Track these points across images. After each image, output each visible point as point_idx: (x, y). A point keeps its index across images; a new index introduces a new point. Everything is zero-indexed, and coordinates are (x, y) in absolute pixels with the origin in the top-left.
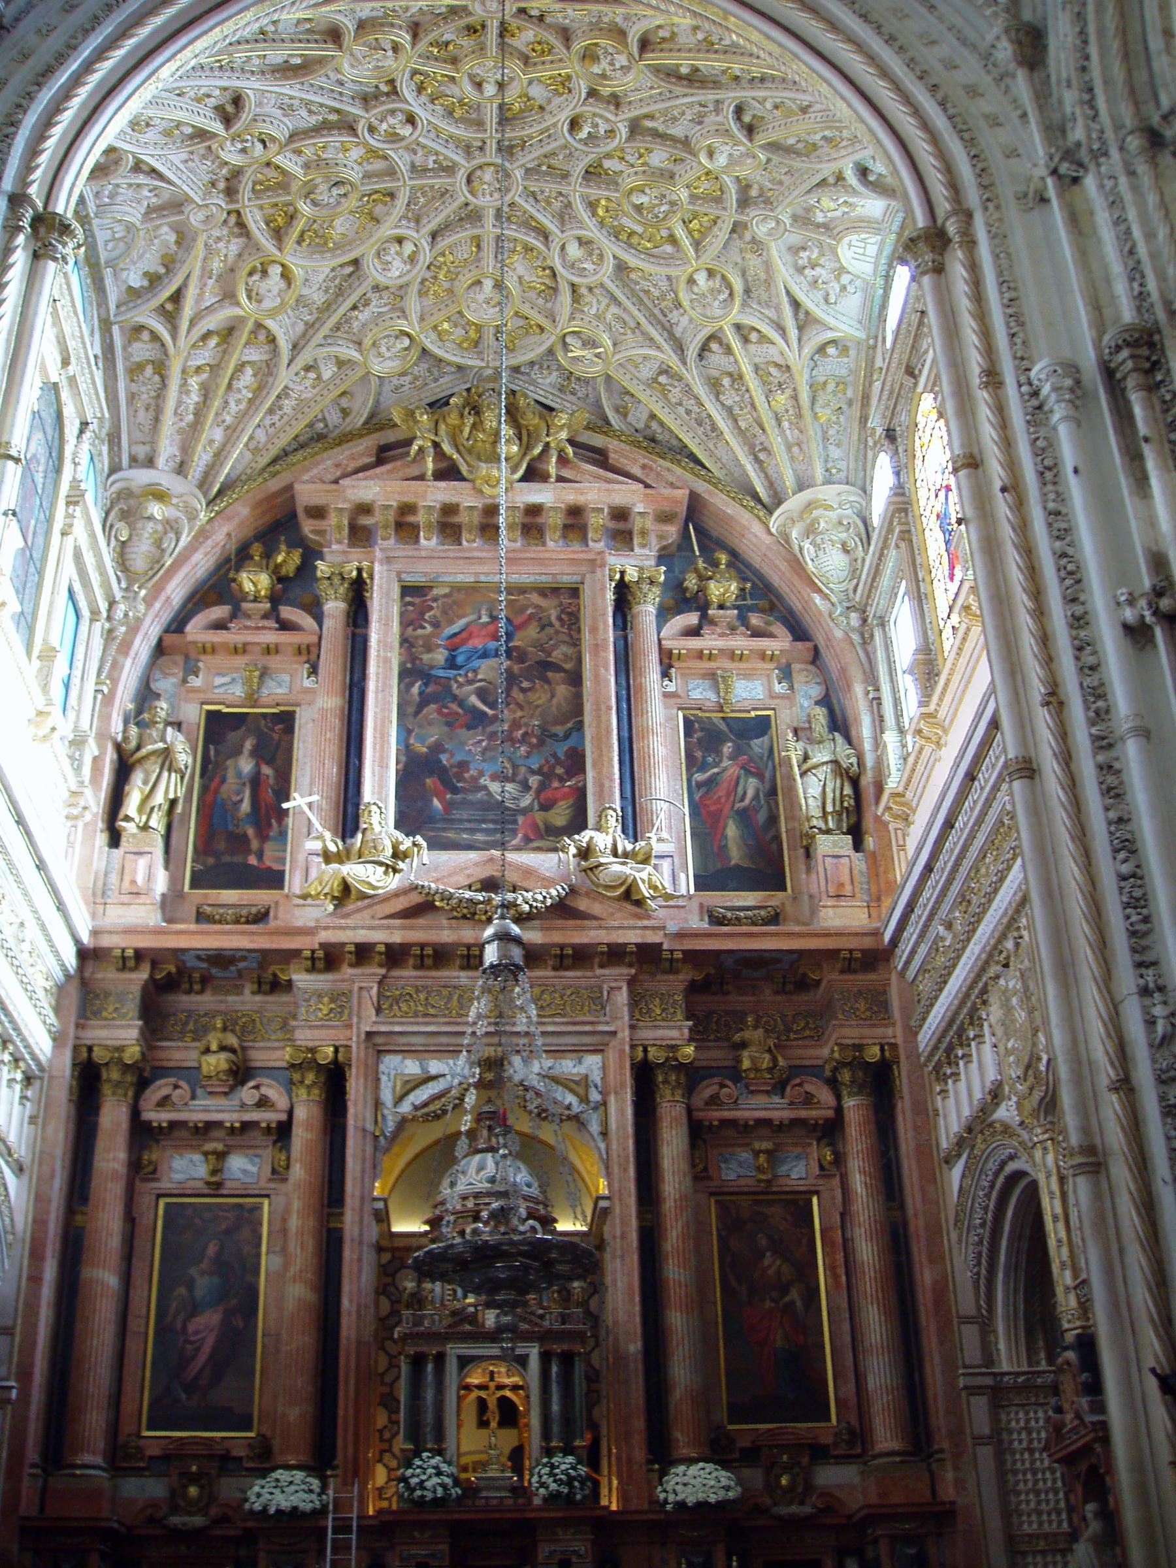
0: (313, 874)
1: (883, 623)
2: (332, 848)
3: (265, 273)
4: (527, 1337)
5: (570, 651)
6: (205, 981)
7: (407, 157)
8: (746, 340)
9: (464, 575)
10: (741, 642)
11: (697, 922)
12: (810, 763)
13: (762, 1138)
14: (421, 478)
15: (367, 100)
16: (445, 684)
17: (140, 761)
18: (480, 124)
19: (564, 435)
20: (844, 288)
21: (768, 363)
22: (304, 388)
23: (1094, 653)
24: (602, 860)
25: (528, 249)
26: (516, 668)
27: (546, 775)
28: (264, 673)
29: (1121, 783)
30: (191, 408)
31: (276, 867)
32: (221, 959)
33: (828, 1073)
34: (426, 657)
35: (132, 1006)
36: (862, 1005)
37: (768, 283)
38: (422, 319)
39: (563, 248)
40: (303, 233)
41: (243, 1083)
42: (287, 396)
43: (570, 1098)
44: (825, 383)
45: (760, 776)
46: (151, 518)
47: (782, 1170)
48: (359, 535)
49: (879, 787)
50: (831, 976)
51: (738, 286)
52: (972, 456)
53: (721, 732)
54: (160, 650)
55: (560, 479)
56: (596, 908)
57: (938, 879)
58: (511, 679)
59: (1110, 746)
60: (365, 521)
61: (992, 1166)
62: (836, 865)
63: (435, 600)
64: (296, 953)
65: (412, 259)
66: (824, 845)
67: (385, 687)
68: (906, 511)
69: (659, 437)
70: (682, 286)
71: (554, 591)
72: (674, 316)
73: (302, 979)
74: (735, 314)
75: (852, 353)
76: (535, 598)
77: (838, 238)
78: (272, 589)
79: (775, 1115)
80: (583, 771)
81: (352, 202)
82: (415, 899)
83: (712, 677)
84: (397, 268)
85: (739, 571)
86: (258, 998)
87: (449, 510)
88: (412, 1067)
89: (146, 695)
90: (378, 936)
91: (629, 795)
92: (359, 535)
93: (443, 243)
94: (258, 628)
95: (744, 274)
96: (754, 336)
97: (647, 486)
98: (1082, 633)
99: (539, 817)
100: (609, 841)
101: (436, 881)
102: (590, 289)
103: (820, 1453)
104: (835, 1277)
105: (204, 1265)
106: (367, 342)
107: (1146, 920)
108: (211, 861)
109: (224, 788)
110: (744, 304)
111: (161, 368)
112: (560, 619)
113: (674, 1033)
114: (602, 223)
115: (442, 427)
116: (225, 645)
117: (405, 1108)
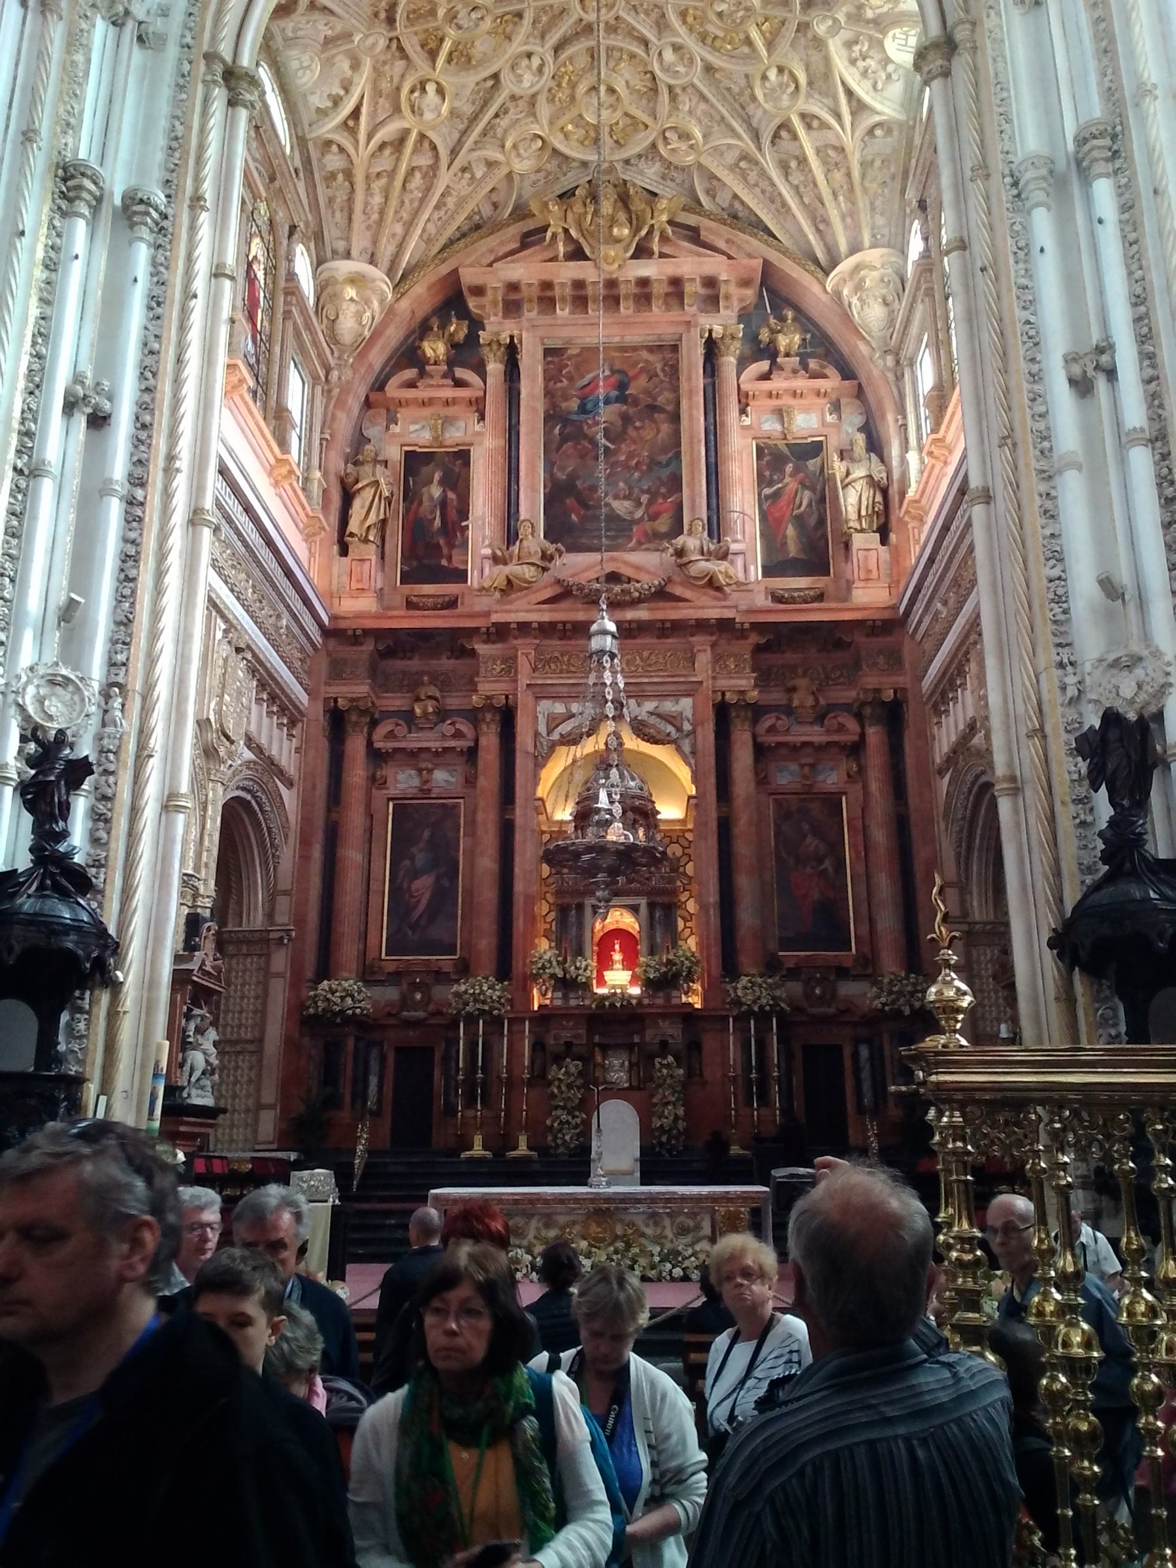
0: (487, 571)
1: (912, 364)
2: (499, 553)
3: (423, 90)
4: (638, 893)
8: (809, 127)
10: (802, 383)
14: (554, 259)
19: (664, 218)
20: (889, 76)
21: (826, 146)
22: (462, 187)
23: (1046, 403)
25: (633, 56)
26: (631, 411)
27: (654, 495)
28: (448, 421)
29: (1056, 507)
30: (376, 208)
31: (461, 567)
32: (423, 636)
33: (855, 709)
34: (564, 405)
36: (881, 660)
37: (827, 74)
38: (551, 123)
39: (660, 54)
40: (450, 54)
41: (443, 721)
42: (449, 194)
43: (670, 729)
44: (873, 161)
45: (813, 489)
46: (352, 300)
47: (820, 778)
48: (512, 308)
49: (903, 494)
50: (860, 639)
51: (802, 79)
52: (962, 240)
54: (368, 404)
55: (662, 255)
56: (687, 594)
57: (939, 567)
58: (626, 419)
59: (1050, 477)
60: (514, 296)
61: (970, 778)
62: (866, 558)
63: (569, 359)
64: (477, 629)
65: (540, 70)
66: (858, 541)
68: (931, 271)
69: (740, 215)
73: (481, 648)
74: (803, 105)
75: (895, 133)
76: (645, 354)
77: (884, 32)
78: (447, 353)
79: (816, 739)
81: (487, 24)
82: (558, 590)
84: (528, 79)
85: (802, 324)
87: (579, 285)
88: (559, 708)
89: (360, 440)
93: (563, 56)
94: (438, 386)
96: (815, 123)
97: (730, 257)
98: (1036, 387)
99: (648, 526)
100: (698, 543)
101: (573, 576)
102: (684, 89)
103: (842, 973)
104: (858, 853)
105: (421, 845)
106: (509, 144)
107: (1065, 612)
108: (415, 564)
109: (422, 509)
110: (809, 96)
111: (349, 174)
112: (663, 370)
113: (743, 682)
115: (570, 215)
117: (555, 736)
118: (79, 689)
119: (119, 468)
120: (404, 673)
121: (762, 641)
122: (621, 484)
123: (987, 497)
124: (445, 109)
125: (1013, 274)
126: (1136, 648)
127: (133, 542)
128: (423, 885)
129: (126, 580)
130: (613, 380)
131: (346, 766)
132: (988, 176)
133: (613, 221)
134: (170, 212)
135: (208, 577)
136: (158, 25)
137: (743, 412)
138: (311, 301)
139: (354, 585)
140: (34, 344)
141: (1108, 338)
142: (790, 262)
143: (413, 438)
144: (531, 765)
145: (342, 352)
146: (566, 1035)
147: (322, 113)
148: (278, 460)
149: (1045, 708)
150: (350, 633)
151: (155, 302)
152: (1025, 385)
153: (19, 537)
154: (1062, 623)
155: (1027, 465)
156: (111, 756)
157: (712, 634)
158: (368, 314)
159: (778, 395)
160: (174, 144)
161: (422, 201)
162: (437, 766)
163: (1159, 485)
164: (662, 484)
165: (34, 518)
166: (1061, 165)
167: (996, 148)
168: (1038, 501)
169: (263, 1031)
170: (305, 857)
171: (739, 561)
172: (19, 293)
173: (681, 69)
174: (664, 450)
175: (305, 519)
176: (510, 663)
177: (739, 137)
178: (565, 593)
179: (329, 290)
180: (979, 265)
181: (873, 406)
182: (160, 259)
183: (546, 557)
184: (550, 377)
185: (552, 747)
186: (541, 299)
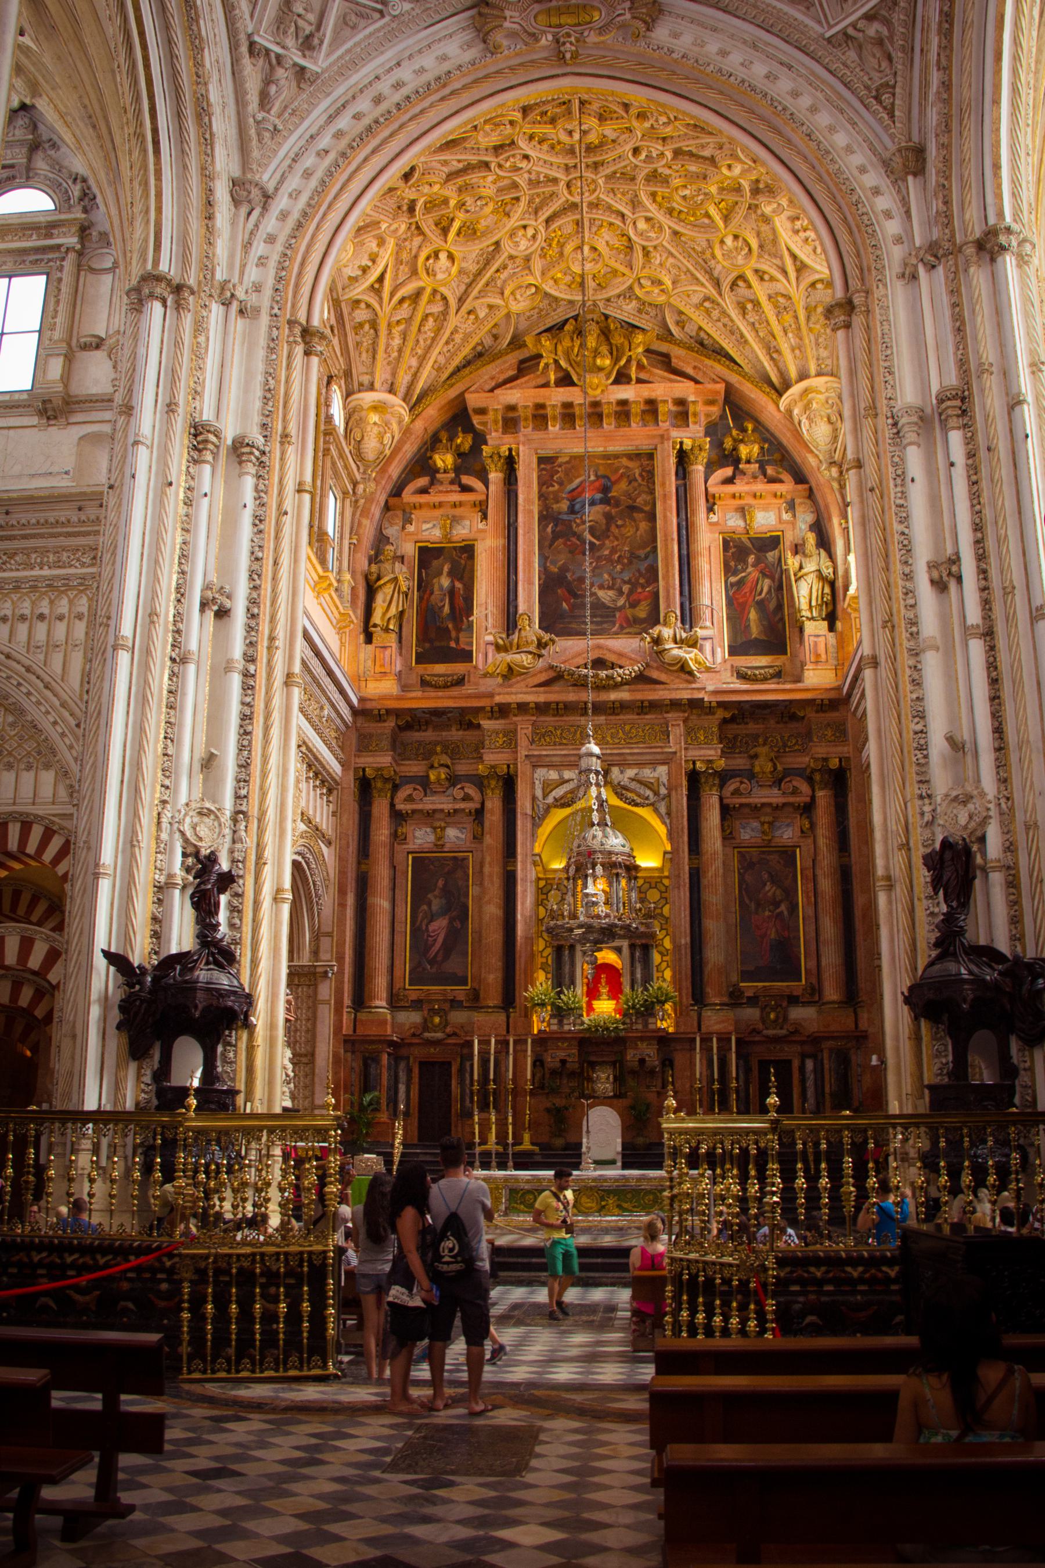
0: (490, 655)
2: (501, 642)
3: (436, 255)
5: (649, 498)
6: (427, 723)
7: (526, 176)
8: (762, 279)
9: (579, 450)
10: (760, 487)
12: (803, 571)
13: (766, 814)
14: (546, 385)
15: (498, 149)
16: (568, 524)
17: (380, 587)
22: (468, 326)
23: (914, 597)
24: (667, 647)
25: (611, 224)
26: (613, 511)
27: (634, 585)
28: (455, 520)
31: (467, 648)
33: (808, 771)
34: (555, 506)
35: (385, 743)
36: (829, 732)
37: (775, 241)
38: (543, 274)
41: (454, 785)
43: (648, 793)
45: (773, 580)
47: (778, 833)
49: (846, 588)
50: (811, 714)
51: (754, 243)
52: (858, 460)
53: (747, 548)
54: (387, 508)
56: (663, 677)
58: (609, 518)
59: (917, 654)
60: (511, 415)
62: (816, 643)
64: (483, 708)
65: (534, 237)
66: (810, 628)
67: (529, 531)
71: (638, 456)
72: (712, 263)
73: (486, 724)
74: (754, 263)
76: (625, 461)
79: (774, 801)
80: (657, 580)
82: (552, 674)
83: (742, 511)
84: (523, 244)
85: (761, 433)
86: (461, 733)
87: (568, 405)
88: (553, 775)
89: (381, 540)
91: (687, 593)
92: (510, 422)
93: (554, 226)
95: (758, 234)
96: (766, 277)
98: (908, 584)
99: (629, 612)
100: (671, 632)
101: (564, 662)
103: (793, 1000)
104: (808, 897)
106: (507, 292)
107: (926, 757)
108: (427, 645)
110: (760, 256)
111: (374, 325)
112: (641, 475)
113: (712, 752)
114: (660, 206)
115: (559, 348)
116: (427, 505)
117: (550, 800)
118: (217, 817)
119: (237, 650)
120: (420, 743)
121: (728, 715)
122: (606, 576)
123: (875, 663)
124: (454, 270)
125: (892, 496)
126: (969, 788)
127: (248, 705)
128: (439, 926)
129: (245, 733)
130: (597, 484)
131: (373, 827)
132: (876, 415)
133: (596, 353)
134: (267, 449)
136: (253, 299)
137: (710, 510)
139: (378, 669)
140: (180, 563)
141: (957, 554)
142: (749, 385)
143: (425, 535)
144: (529, 825)
145: (367, 467)
146: (562, 1054)
147: (354, 279)
148: (320, 577)
149: (910, 827)
151: (258, 520)
152: (900, 583)
154: (923, 766)
156: (240, 865)
158: (388, 435)
159: (740, 497)
160: (269, 396)
161: (433, 339)
162: (448, 825)
163: (988, 668)
164: (641, 575)
165: (184, 694)
167: (882, 394)
168: (908, 672)
169: (314, 1047)
170: (342, 905)
171: (708, 646)
172: (170, 530)
173: (653, 235)
177: (703, 285)
178: (556, 677)
179: (356, 416)
180: (869, 485)
182: (261, 487)
183: (541, 645)
184: (544, 482)
185: (548, 810)
186: (535, 416)
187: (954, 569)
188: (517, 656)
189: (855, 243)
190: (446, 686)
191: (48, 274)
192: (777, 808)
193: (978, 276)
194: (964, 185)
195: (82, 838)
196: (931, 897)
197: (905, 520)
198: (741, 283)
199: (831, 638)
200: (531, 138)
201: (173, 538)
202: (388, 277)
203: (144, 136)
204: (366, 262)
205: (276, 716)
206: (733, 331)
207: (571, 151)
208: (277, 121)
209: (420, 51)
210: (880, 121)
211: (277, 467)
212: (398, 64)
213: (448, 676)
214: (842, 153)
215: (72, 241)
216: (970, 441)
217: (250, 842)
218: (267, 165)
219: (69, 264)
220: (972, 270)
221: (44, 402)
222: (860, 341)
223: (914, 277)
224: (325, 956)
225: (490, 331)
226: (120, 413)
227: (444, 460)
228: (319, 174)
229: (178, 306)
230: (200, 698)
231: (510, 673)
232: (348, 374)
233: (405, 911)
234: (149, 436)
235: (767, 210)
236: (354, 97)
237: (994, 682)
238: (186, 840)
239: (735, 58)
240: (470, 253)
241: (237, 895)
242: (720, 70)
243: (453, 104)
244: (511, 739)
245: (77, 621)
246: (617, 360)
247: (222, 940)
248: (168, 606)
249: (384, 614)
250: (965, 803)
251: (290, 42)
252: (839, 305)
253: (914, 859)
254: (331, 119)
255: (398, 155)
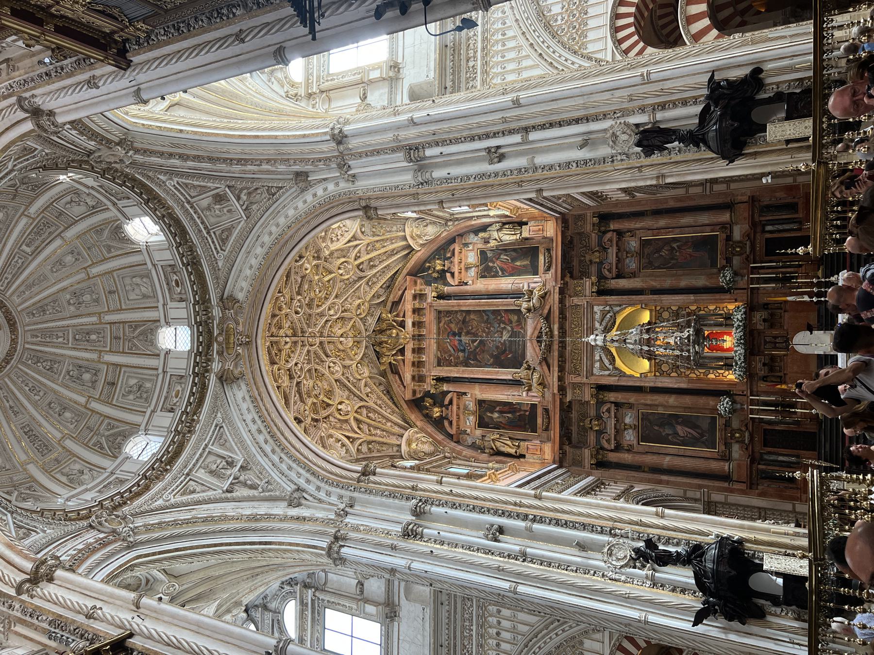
0: (533, 394)
1: (453, 214)
3: (340, 410)
7: (305, 365)
8: (359, 257)
9: (434, 347)
10: (456, 260)
11: (549, 275)
13: (622, 255)
14: (404, 361)
15: (291, 377)
18: (295, 343)
25: (331, 327)
27: (501, 322)
28: (466, 408)
33: (599, 234)
35: (578, 452)
37: (342, 250)
38: (352, 360)
43: (608, 316)
45: (500, 254)
47: (633, 249)
49: (507, 216)
50: (569, 233)
51: (343, 260)
52: (439, 202)
54: (458, 442)
56: (547, 307)
58: (468, 333)
60: (417, 378)
64: (560, 399)
65: (334, 363)
66: (525, 234)
67: (472, 372)
70: (343, 277)
73: (568, 399)
74: (352, 260)
76: (441, 325)
78: (438, 407)
81: (320, 384)
82: (544, 363)
83: (467, 268)
84: (337, 368)
87: (414, 351)
88: (597, 365)
89: (474, 446)
90: (556, 375)
95: (339, 258)
96: (358, 255)
97: (406, 289)
98: (500, 174)
99: (514, 324)
100: (524, 303)
101: (538, 357)
104: (669, 232)
105: (662, 430)
106: (359, 378)
107: (591, 160)
108: (527, 426)
110: (348, 257)
113: (588, 283)
114: (323, 303)
115: (387, 354)
116: (458, 422)
117: (611, 367)
118: (613, 545)
119: (521, 524)
120: (578, 434)
123: (540, 191)
124: (347, 402)
129: (566, 524)
131: (623, 462)
133: (390, 336)
135: (565, 495)
138: (417, 462)
140: (473, 551)
143: (472, 424)
144: (624, 379)
145: (438, 451)
147: (347, 451)
148: (489, 478)
149: (629, 166)
150: (561, 455)
151: (454, 506)
153: (551, 563)
154: (595, 161)
155: (531, 177)
157: (565, 297)
160: (393, 495)
161: (379, 414)
162: (623, 422)
164: (496, 318)
165: (543, 556)
166: (416, 167)
168: (545, 172)
170: (668, 483)
171: (532, 285)
174: (482, 317)
175: (510, 471)
176: (576, 386)
177: (361, 285)
178: (545, 361)
179: (413, 454)
180: (451, 196)
181: (467, 229)
183: (529, 368)
185: (617, 369)
186: (418, 367)
187: (493, 150)
188: (534, 380)
189: (338, 205)
190: (549, 418)
191: (325, 608)
192: (619, 250)
193: (353, 143)
194: (312, 152)
195: (623, 628)
196: (670, 152)
197: (468, 177)
198: (361, 267)
199: (530, 224)
200: (287, 361)
201: (460, 553)
202: (347, 434)
203: (263, 549)
204: (339, 444)
205: (557, 506)
206: (383, 272)
207: (295, 343)
208: (264, 481)
209: (240, 410)
210: (283, 193)
211: (428, 494)
212: (244, 420)
213: (543, 417)
214: (297, 212)
215: (310, 592)
216: (430, 145)
217: (628, 528)
218: (284, 488)
219: (321, 596)
220: (350, 146)
221: (387, 617)
222: (383, 203)
223: (354, 176)
224: (698, 495)
225: (377, 387)
226: (394, 576)
227: (436, 412)
228: (290, 462)
229: (345, 539)
230: (545, 547)
231: (542, 384)
232: (392, 457)
233: (672, 448)
234: (407, 561)
235: (327, 253)
236: (257, 443)
237: (551, 125)
238: (626, 565)
239: (254, 262)
240: (340, 394)
241: (659, 539)
242: (258, 269)
243: (265, 395)
244: (580, 386)
245: (501, 614)
246: (394, 326)
247: (687, 551)
248: (495, 560)
249: (510, 447)
250: (617, 137)
251: (228, 472)
252: (366, 213)
253: (647, 163)
254: (266, 455)
255: (286, 423)
